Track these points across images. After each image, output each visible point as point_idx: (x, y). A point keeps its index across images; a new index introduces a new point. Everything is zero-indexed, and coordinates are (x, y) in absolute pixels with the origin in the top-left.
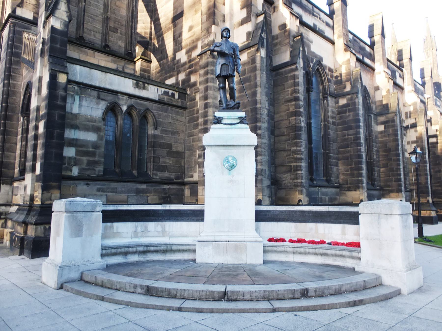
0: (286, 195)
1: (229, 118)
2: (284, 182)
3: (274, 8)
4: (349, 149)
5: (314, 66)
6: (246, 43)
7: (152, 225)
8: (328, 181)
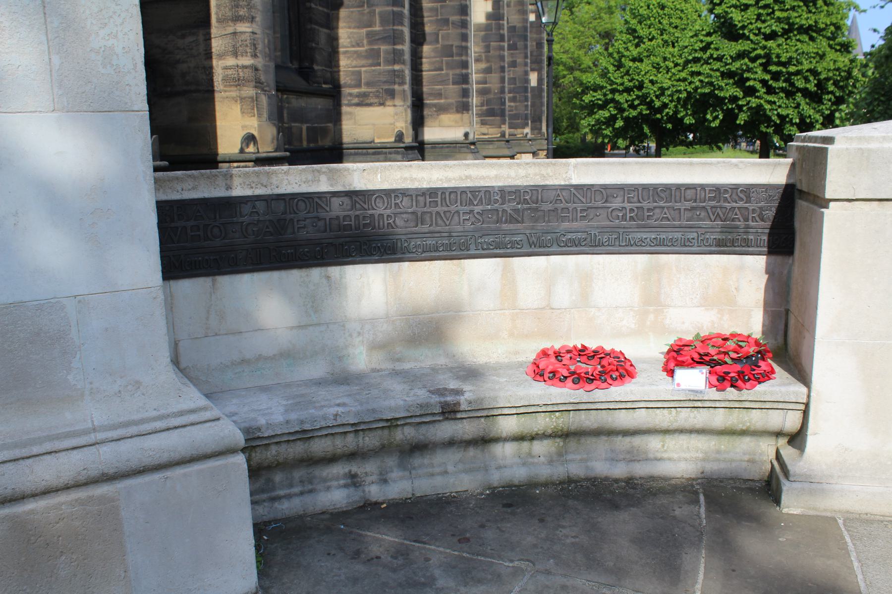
2: (183, 67)
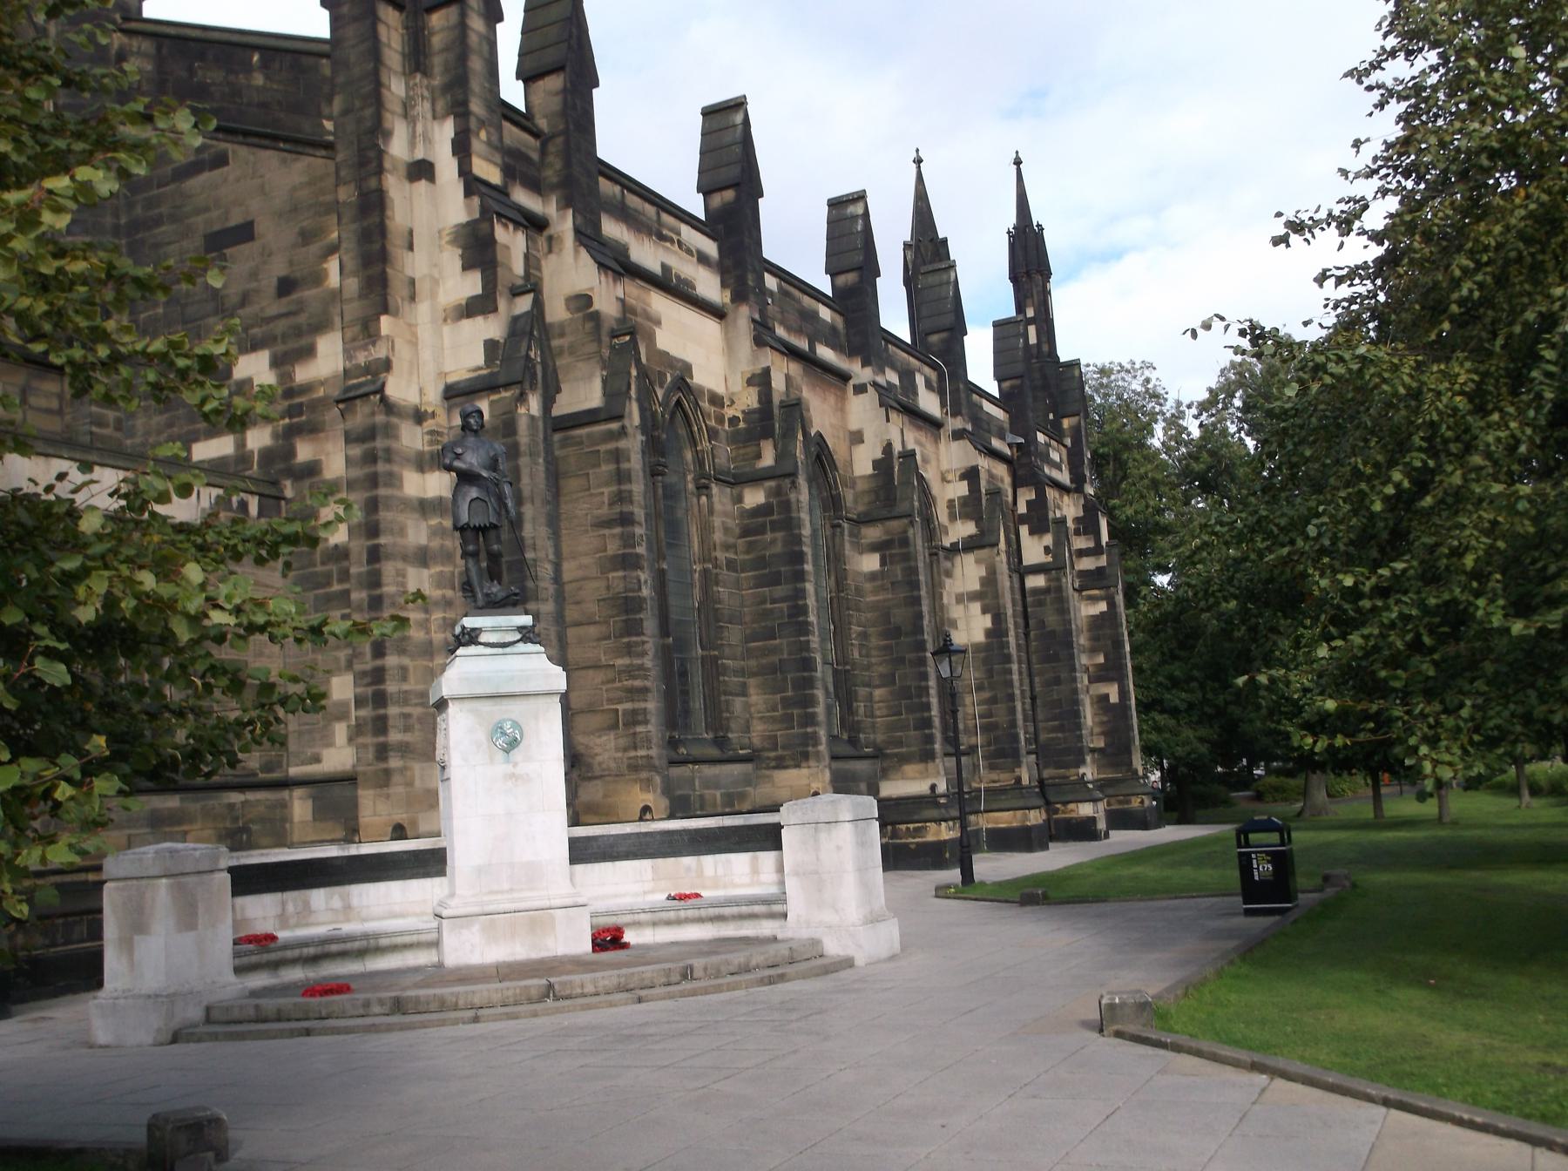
0: (605, 796)
1: (494, 630)
2: (599, 759)
3: (550, 239)
4: (777, 641)
5: (667, 396)
6: (484, 372)
7: (319, 897)
8: (721, 742)
